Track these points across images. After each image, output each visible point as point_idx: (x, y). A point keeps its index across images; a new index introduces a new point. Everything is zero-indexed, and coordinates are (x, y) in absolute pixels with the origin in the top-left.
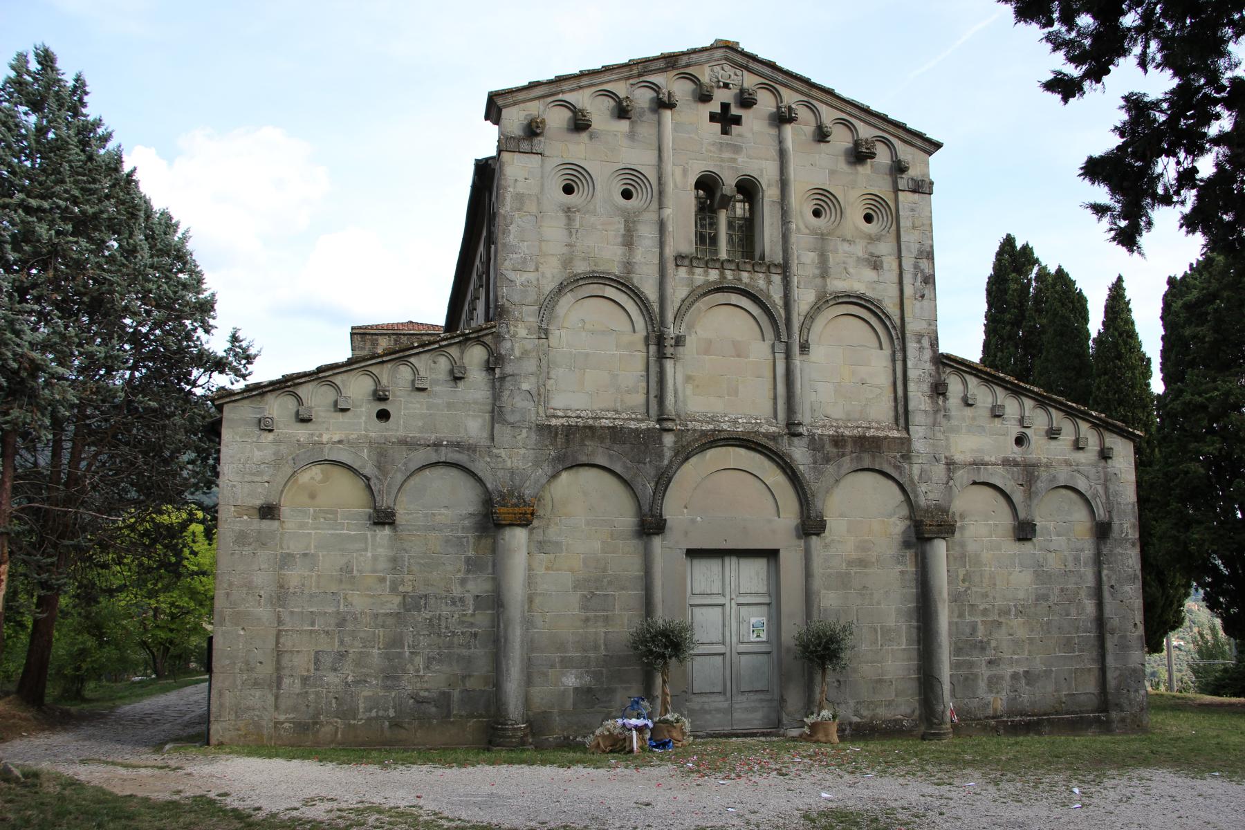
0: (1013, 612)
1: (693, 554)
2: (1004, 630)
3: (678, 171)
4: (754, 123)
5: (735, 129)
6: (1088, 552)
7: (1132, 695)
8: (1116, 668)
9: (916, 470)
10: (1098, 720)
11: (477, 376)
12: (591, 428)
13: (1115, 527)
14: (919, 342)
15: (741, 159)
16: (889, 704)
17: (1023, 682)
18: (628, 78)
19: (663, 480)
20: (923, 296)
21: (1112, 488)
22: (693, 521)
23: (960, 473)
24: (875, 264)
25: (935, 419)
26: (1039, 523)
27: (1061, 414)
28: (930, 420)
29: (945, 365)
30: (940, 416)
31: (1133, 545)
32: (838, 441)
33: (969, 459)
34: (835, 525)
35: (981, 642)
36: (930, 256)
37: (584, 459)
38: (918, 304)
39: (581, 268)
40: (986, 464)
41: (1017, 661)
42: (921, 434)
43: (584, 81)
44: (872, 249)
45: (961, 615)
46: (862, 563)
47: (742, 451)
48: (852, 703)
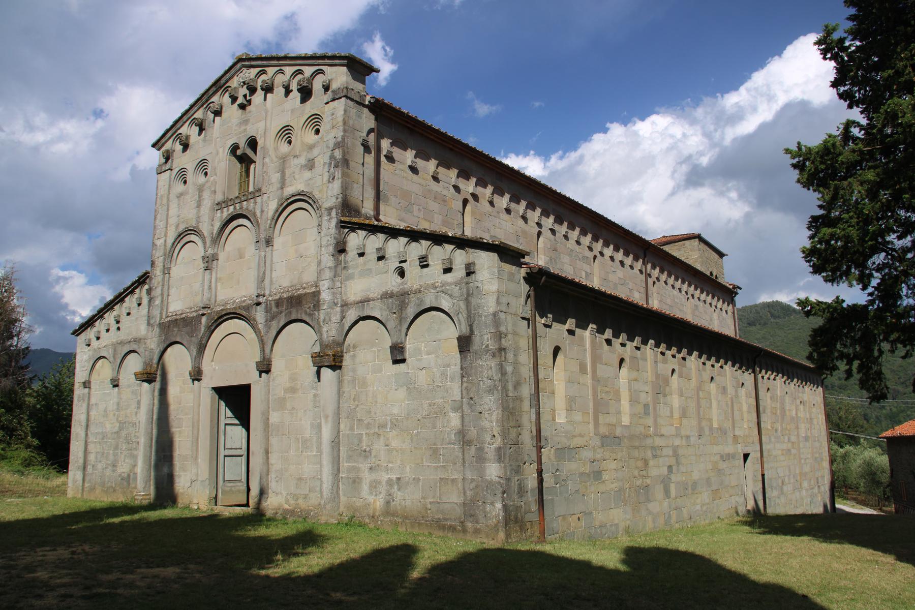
0: (389, 426)
2: (382, 438)
3: (221, 150)
5: (248, 108)
6: (455, 368)
7: (488, 508)
8: (473, 480)
9: (322, 316)
11: (145, 301)
12: (176, 320)
13: (476, 339)
14: (330, 214)
17: (396, 487)
18: (202, 106)
19: (202, 348)
20: (333, 179)
21: (473, 301)
22: (214, 369)
23: (350, 312)
24: (310, 165)
25: (336, 271)
26: (409, 347)
28: (332, 274)
31: (494, 355)
32: (278, 303)
34: (277, 365)
35: (365, 451)
38: (330, 185)
39: (182, 228)
40: (368, 300)
41: (392, 469)
42: (326, 286)
43: (185, 118)
45: (352, 429)
46: (293, 390)
48: (284, 493)
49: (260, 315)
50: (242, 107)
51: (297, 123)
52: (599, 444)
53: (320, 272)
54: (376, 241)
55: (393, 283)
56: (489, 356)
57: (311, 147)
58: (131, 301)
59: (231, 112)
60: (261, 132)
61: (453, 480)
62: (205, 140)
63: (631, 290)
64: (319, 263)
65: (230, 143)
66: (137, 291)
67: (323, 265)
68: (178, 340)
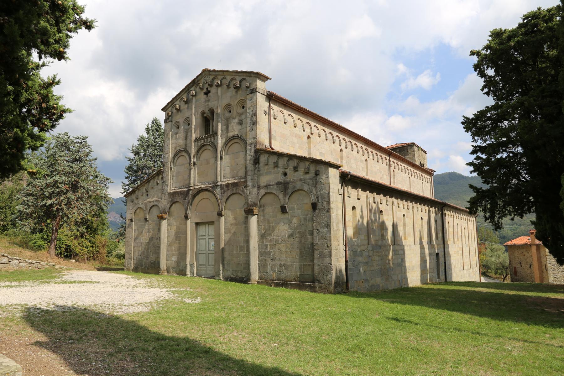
1: (197, 224)
4: (213, 90)
5: (209, 94)
7: (325, 277)
8: (319, 265)
9: (248, 192)
10: (310, 286)
12: (177, 192)
15: (209, 103)
16: (241, 272)
27: (298, 161)
28: (253, 173)
29: (258, 152)
30: (256, 171)
32: (227, 185)
33: (265, 184)
36: (255, 114)
37: (175, 200)
39: (178, 148)
40: (270, 185)
43: (178, 98)
44: (240, 118)
47: (207, 192)
49: (218, 191)
50: (207, 93)
51: (234, 103)
52: (371, 249)
53: (246, 172)
54: (273, 159)
55: (281, 178)
56: (325, 212)
57: (241, 115)
58: (153, 183)
59: (202, 96)
60: (216, 106)
61: (309, 265)
62: (188, 108)
63: (383, 175)
64: (246, 168)
65: (200, 110)
66: (157, 177)
67: (248, 169)
68: (178, 200)
